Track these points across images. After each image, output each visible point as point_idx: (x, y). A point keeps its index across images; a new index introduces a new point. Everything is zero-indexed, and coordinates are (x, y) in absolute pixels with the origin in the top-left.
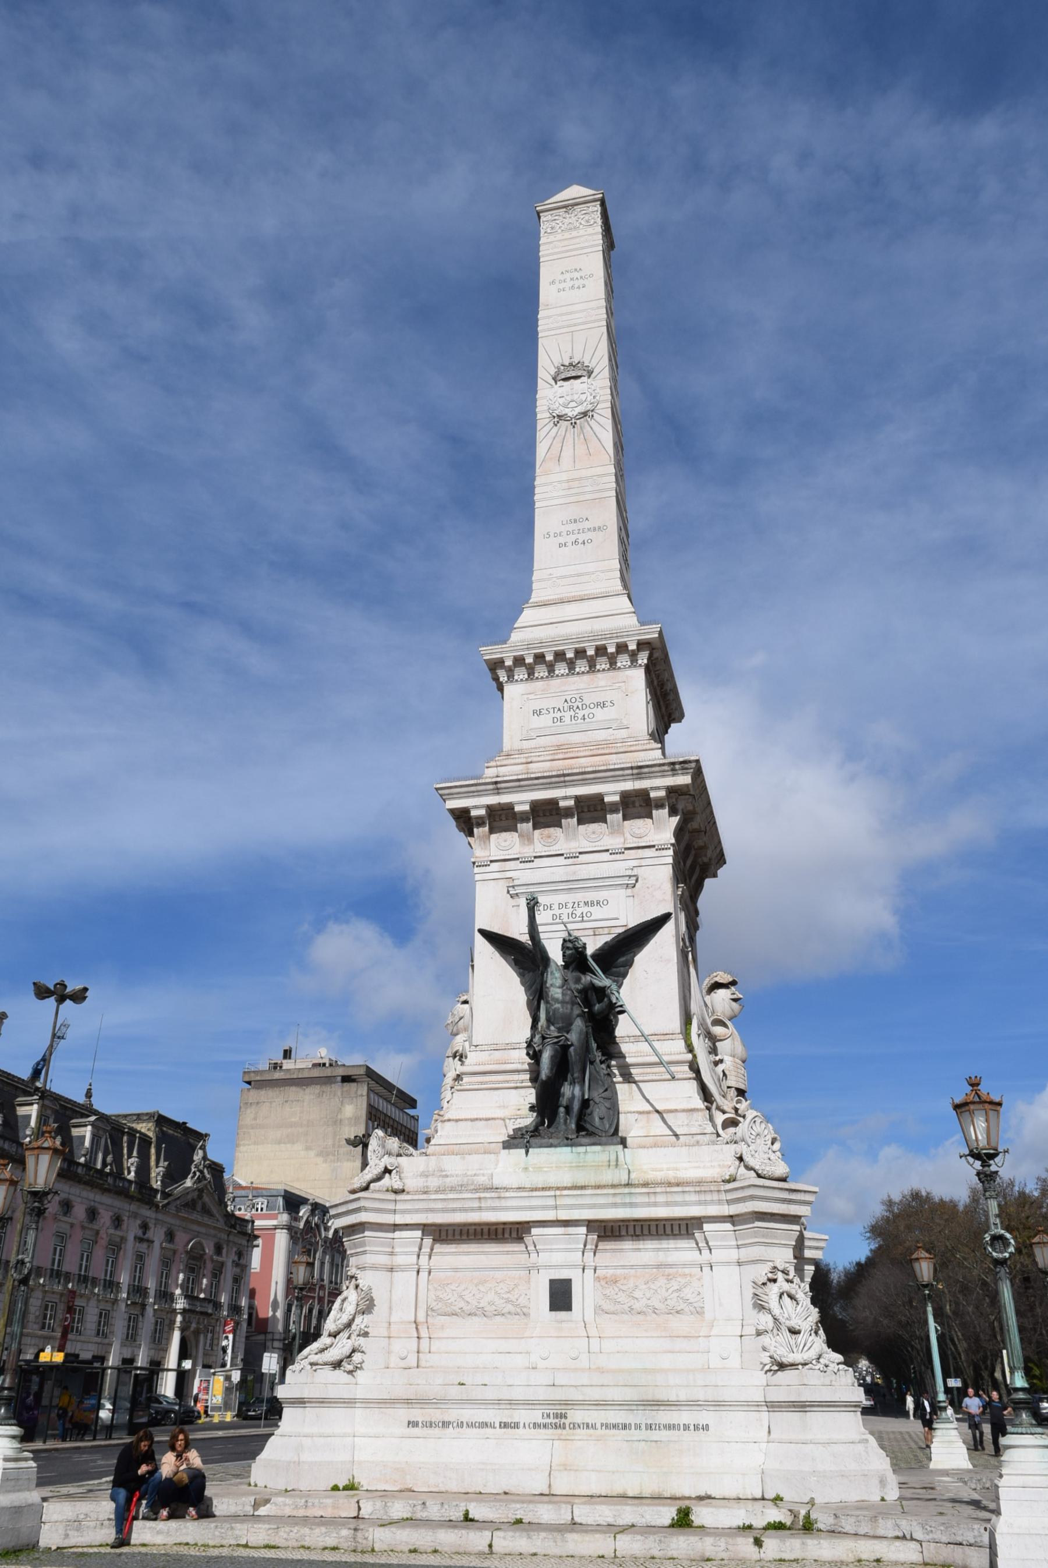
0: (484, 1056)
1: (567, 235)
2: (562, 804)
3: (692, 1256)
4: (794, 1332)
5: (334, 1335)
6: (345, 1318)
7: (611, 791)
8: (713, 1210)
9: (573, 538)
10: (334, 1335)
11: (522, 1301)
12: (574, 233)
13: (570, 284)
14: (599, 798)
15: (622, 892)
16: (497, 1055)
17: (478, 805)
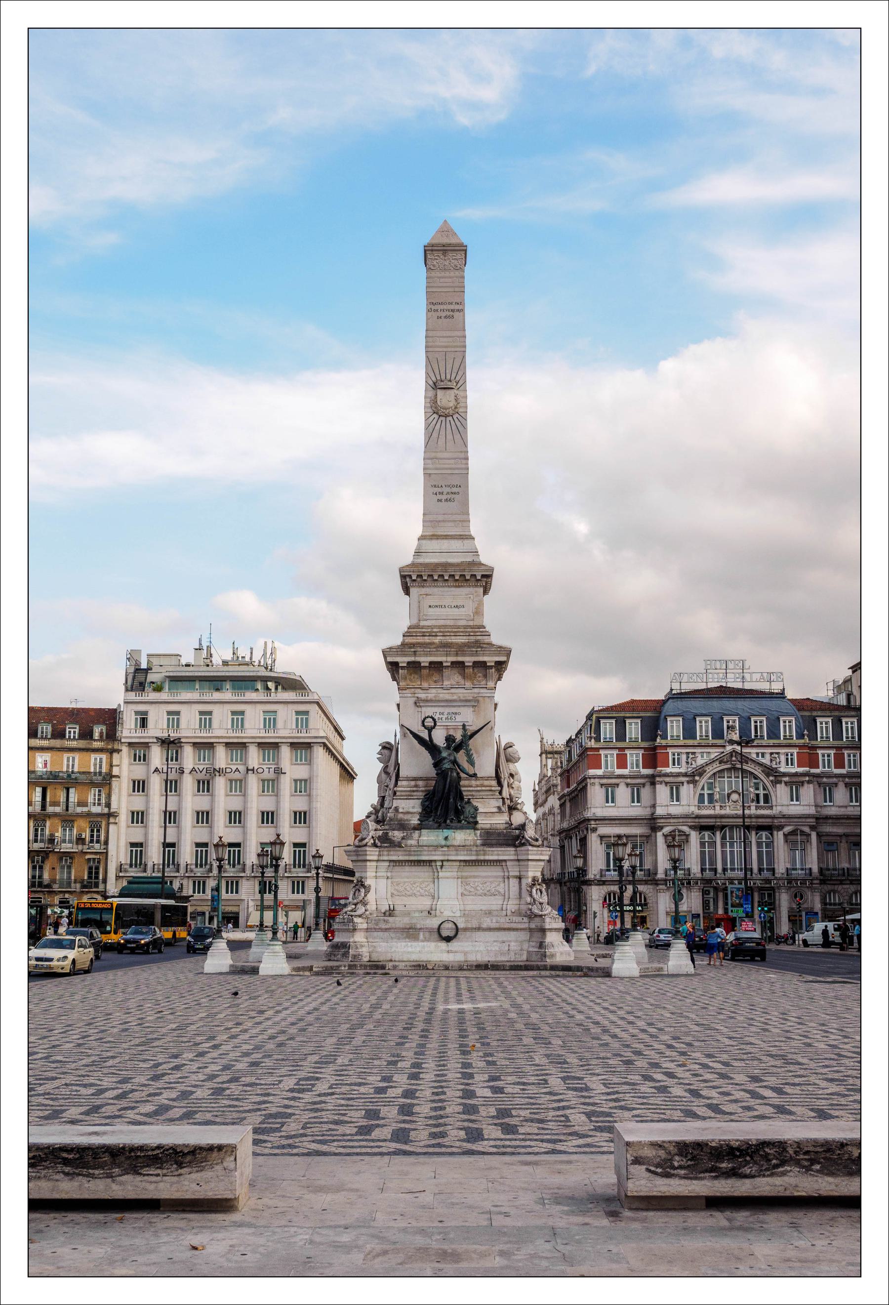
0: (405, 783)
1: (443, 274)
2: (444, 664)
3: (502, 874)
4: (541, 904)
5: (356, 905)
6: (361, 898)
7: (468, 660)
8: (512, 858)
9: (444, 497)
10: (356, 905)
11: (432, 891)
12: (447, 274)
13: (444, 314)
14: (463, 663)
15: (472, 709)
16: (413, 783)
17: (403, 660)
